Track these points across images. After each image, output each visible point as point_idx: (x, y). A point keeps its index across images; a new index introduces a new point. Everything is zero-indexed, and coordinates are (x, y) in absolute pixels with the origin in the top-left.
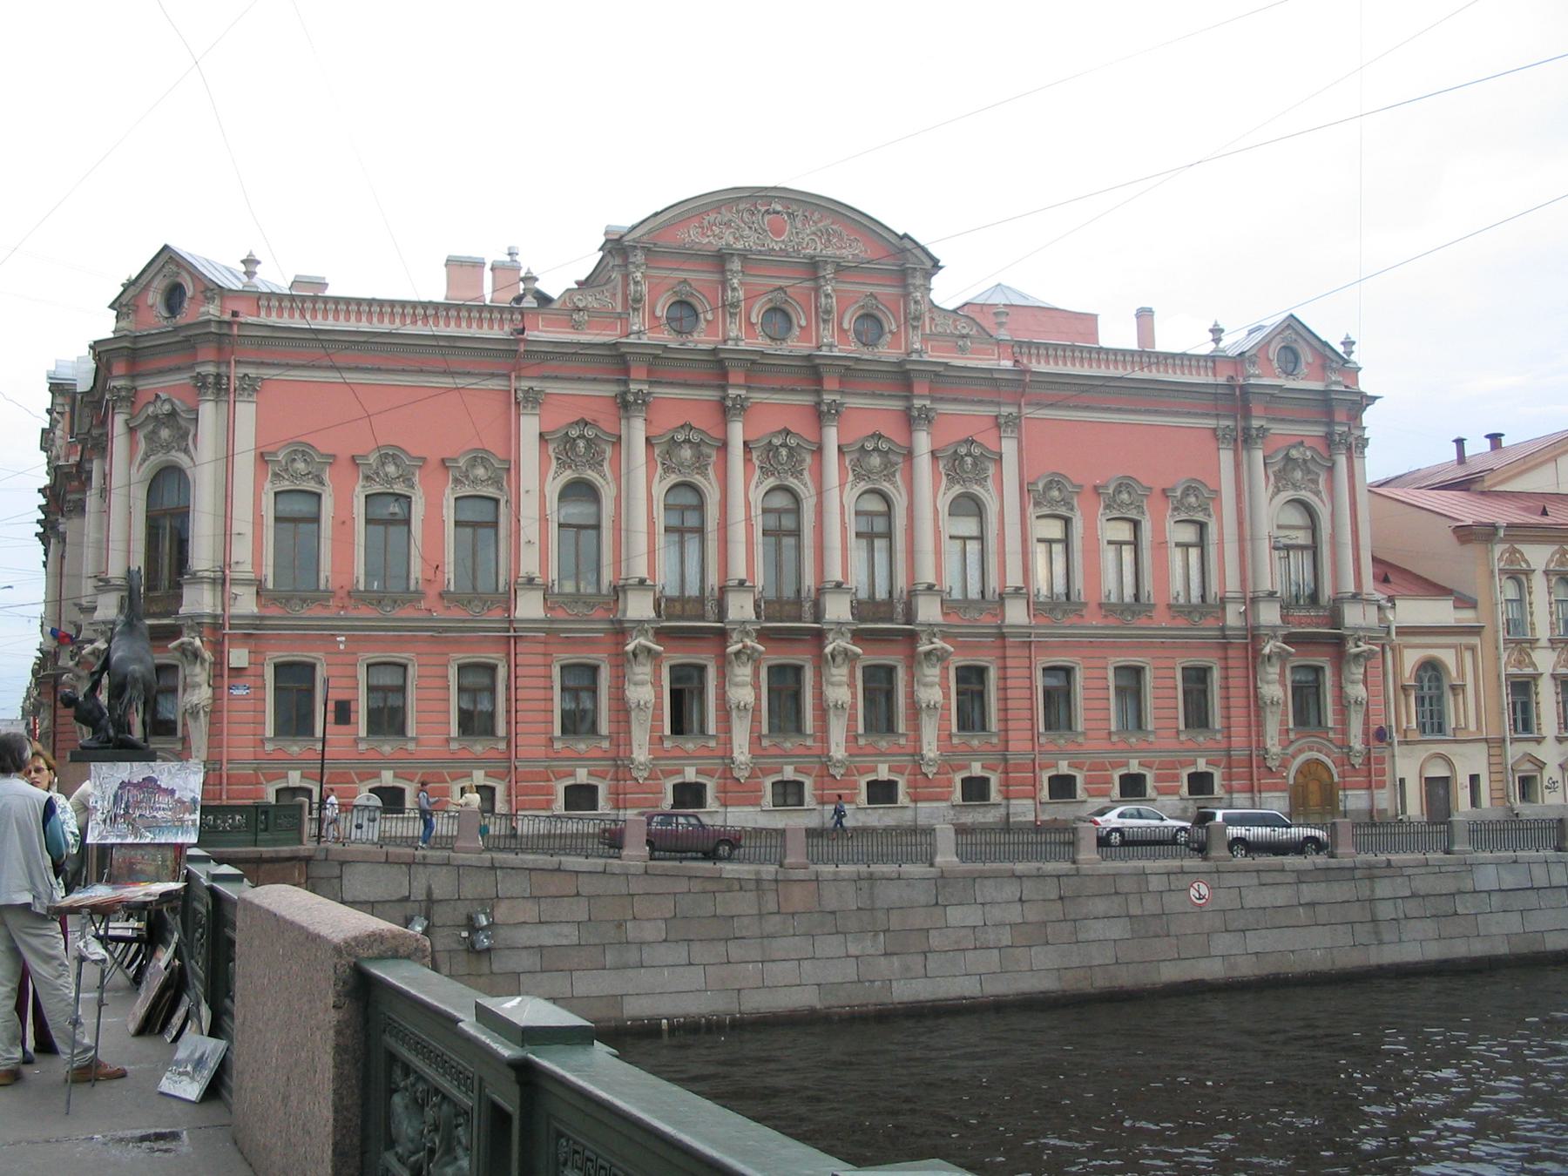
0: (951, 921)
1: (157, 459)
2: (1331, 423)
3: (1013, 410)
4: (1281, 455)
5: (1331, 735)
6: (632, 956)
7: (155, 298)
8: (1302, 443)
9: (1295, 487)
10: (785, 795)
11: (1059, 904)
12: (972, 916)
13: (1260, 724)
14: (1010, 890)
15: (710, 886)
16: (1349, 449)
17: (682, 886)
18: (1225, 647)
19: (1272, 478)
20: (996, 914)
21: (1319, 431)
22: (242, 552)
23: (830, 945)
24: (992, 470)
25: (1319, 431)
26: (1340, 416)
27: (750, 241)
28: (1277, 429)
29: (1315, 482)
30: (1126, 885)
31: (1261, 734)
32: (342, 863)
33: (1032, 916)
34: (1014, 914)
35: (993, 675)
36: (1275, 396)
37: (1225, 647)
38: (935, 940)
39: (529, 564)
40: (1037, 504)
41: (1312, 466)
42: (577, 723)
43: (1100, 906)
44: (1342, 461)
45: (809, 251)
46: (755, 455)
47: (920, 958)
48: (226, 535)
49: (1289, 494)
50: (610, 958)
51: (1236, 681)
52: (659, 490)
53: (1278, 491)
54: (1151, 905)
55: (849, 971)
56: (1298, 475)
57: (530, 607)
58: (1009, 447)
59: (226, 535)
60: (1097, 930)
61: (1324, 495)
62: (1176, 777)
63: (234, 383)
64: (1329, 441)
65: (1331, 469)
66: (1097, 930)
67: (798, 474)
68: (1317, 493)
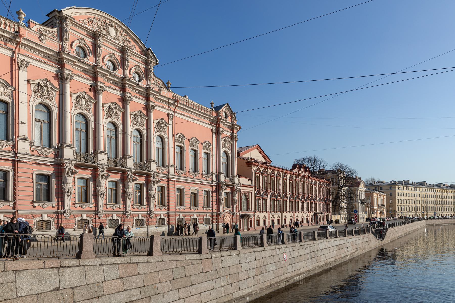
35: (166, 189)
37: (212, 186)
39: (23, 130)
51: (214, 195)
61: (230, 151)
67: (118, 119)
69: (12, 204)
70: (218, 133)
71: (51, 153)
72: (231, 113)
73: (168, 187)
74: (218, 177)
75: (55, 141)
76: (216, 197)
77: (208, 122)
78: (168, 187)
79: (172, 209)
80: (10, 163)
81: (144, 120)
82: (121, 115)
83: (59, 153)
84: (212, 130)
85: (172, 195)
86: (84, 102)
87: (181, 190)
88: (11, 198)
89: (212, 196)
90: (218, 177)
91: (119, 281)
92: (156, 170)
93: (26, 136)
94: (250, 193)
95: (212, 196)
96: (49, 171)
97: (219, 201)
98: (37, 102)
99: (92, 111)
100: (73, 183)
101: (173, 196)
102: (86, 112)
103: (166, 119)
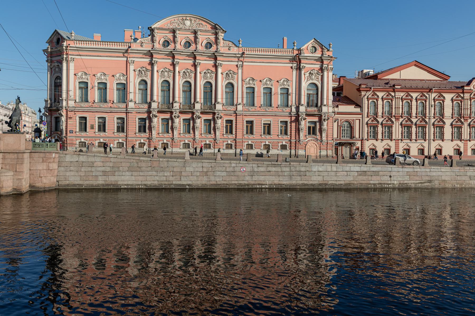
0: (187, 170)
1: (56, 75)
3: (241, 63)
5: (318, 137)
6: (120, 173)
7: (55, 40)
10: (185, 146)
11: (211, 168)
12: (192, 169)
13: (299, 135)
14: (200, 165)
15: (137, 161)
17: (132, 161)
18: (291, 116)
20: (197, 169)
22: (71, 93)
23: (161, 174)
24: (236, 76)
26: (325, 62)
27: (181, 26)
28: (307, 66)
30: (226, 165)
31: (299, 137)
32: (66, 154)
33: (205, 170)
34: (201, 170)
35: (234, 122)
38: (183, 174)
39: (131, 96)
40: (246, 84)
42: (142, 129)
43: (220, 169)
45: (194, 29)
46: (181, 74)
47: (179, 177)
48: (68, 91)
49: (311, 81)
50: (116, 173)
51: (293, 124)
52: (160, 81)
54: (231, 169)
55: (164, 178)
57: (131, 105)
58: (240, 71)
59: (68, 91)
60: (218, 173)
61: (320, 83)
62: (278, 146)
63: (70, 59)
64: (322, 69)
65: (322, 77)
66: (218, 173)
68: (318, 81)
69: (125, 134)
70: (299, 69)
71: (146, 106)
72: (321, 46)
73: (236, 120)
74: (297, 108)
75: (149, 100)
76: (296, 126)
77: (288, 61)
78: (236, 120)
79: (239, 136)
80: (125, 114)
81: (212, 74)
82: (193, 75)
83: (150, 106)
84: (292, 67)
85: (239, 126)
86: (166, 73)
87: (251, 122)
88: (125, 132)
89: (291, 126)
90: (297, 108)
91: (101, 163)
92: (221, 109)
93: (133, 99)
94: (358, 121)
95: (291, 126)
96: (145, 116)
97: (298, 130)
98: (140, 79)
99: (171, 78)
100: (157, 122)
101: (241, 126)
102: (168, 79)
103: (235, 69)
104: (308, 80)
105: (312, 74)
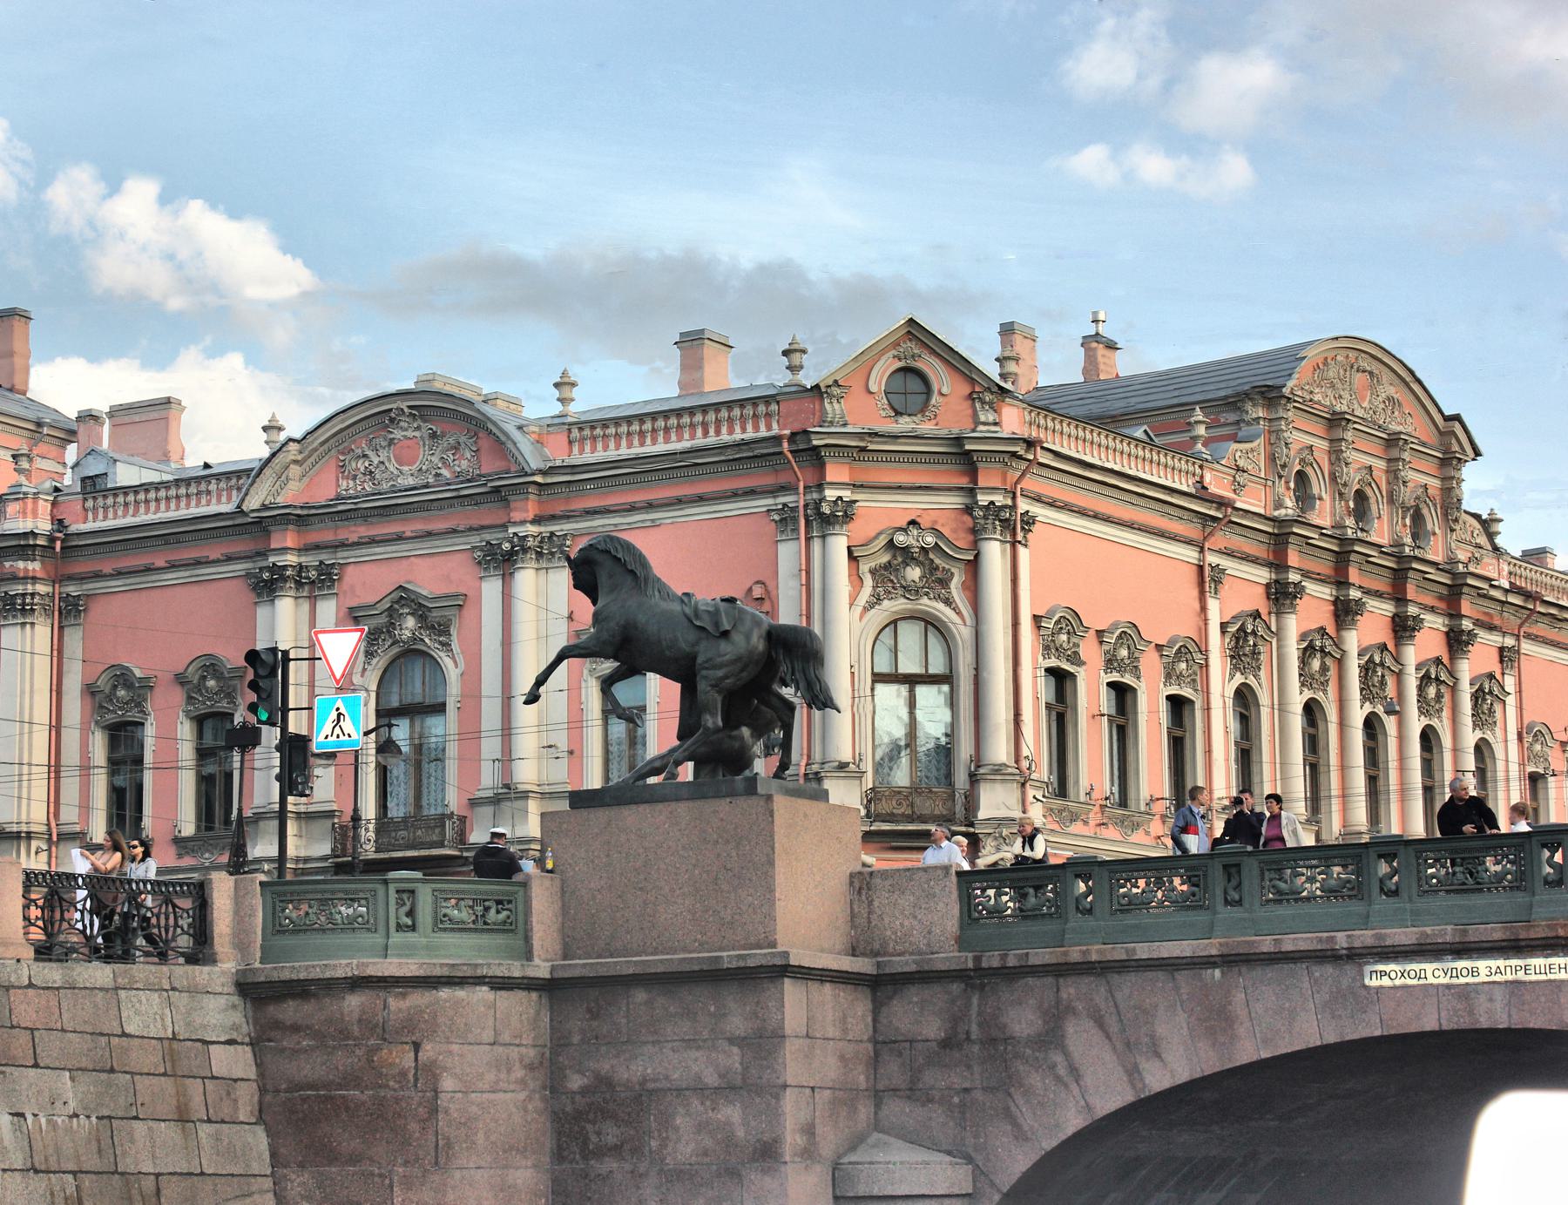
2: (971, 492)
4: (883, 540)
8: (913, 523)
9: (910, 591)
16: (1008, 525)
19: (868, 581)
21: (954, 501)
25: (954, 501)
29: (944, 583)
36: (861, 450)
41: (937, 561)
44: (994, 553)
53: (876, 600)
56: (914, 573)
65: (974, 566)
68: (948, 602)
104: (876, 600)
105: (906, 550)
